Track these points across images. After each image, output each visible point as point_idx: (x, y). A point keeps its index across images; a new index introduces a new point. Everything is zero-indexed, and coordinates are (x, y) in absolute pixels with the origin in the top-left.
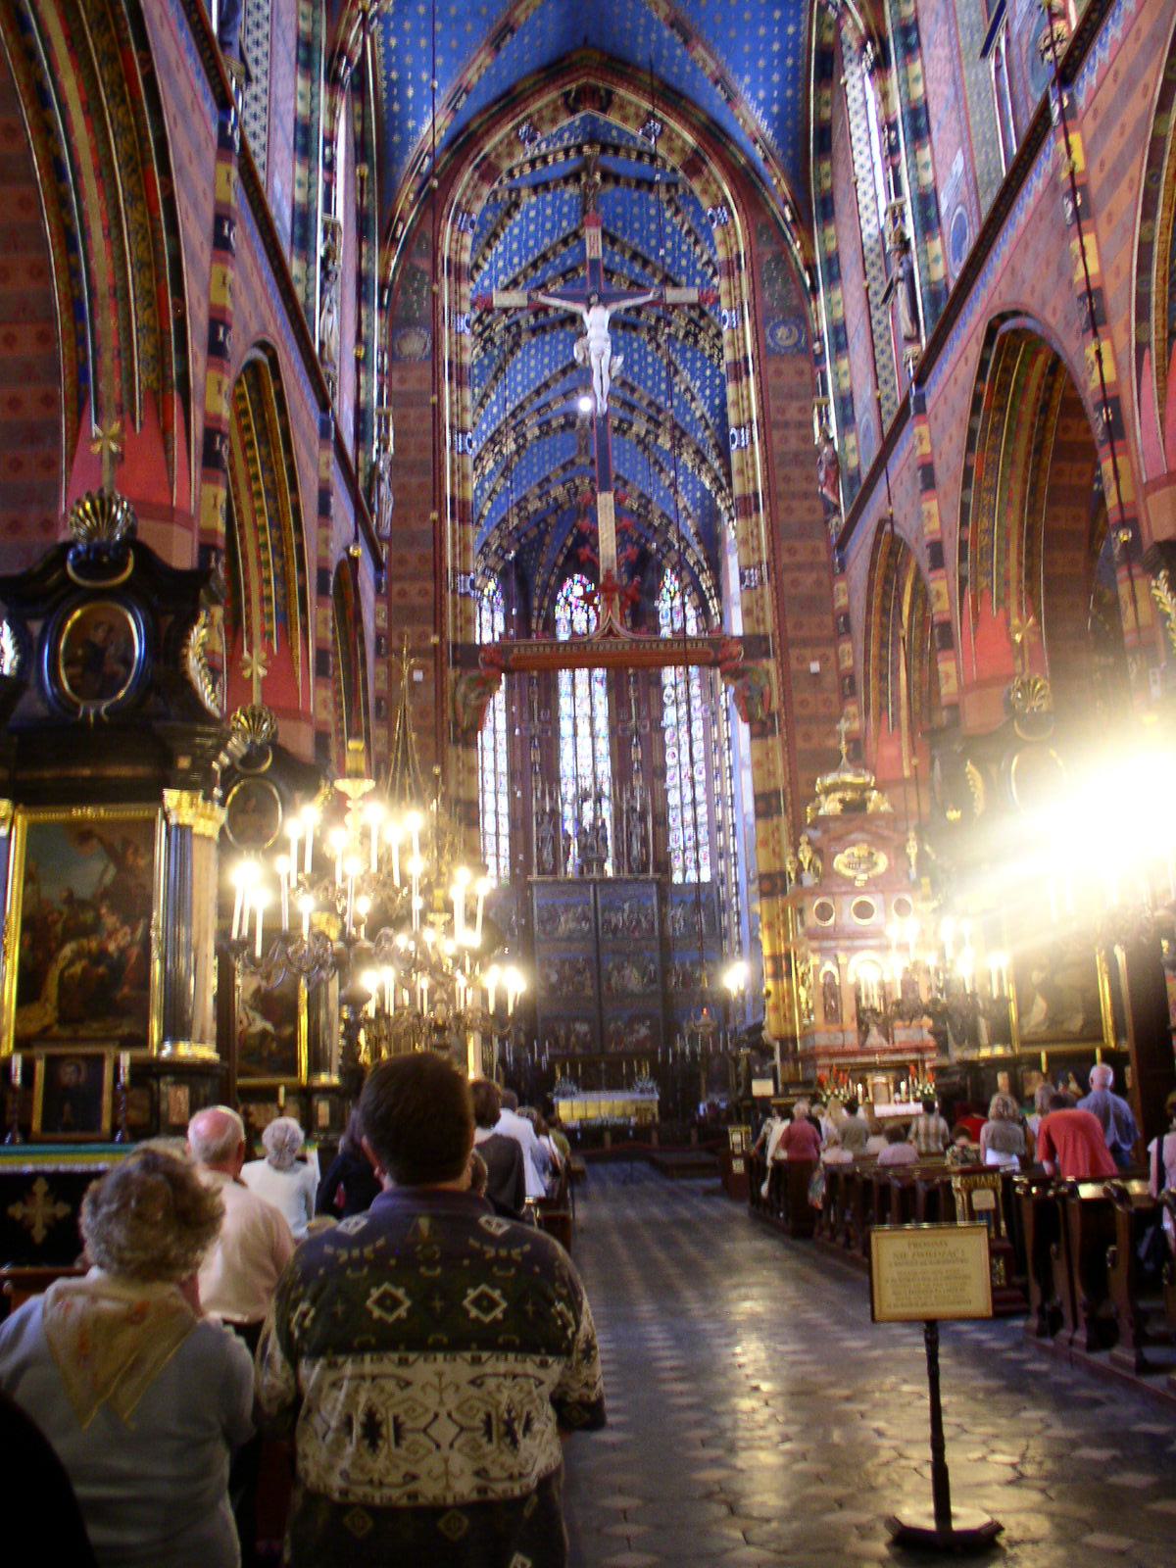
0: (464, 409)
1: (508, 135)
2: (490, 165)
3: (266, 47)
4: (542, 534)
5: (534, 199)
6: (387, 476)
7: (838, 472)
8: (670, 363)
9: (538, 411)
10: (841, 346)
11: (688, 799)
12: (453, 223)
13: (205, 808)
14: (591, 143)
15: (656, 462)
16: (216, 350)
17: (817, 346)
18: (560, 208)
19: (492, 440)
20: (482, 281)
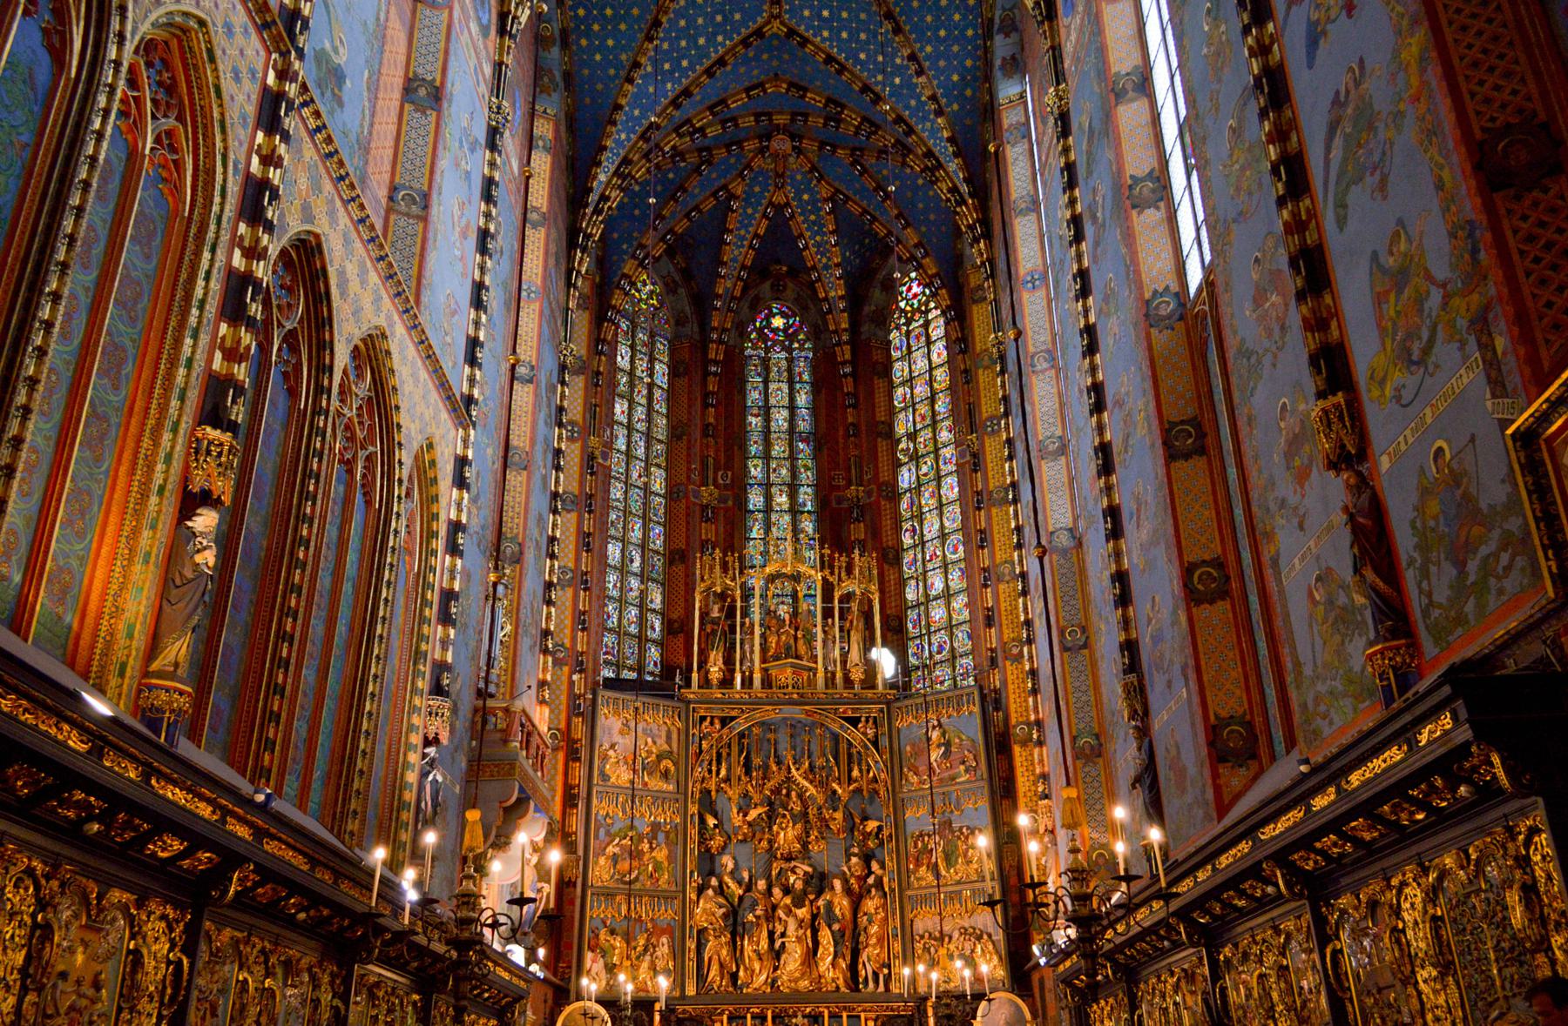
11: (938, 585)
15: (889, 16)
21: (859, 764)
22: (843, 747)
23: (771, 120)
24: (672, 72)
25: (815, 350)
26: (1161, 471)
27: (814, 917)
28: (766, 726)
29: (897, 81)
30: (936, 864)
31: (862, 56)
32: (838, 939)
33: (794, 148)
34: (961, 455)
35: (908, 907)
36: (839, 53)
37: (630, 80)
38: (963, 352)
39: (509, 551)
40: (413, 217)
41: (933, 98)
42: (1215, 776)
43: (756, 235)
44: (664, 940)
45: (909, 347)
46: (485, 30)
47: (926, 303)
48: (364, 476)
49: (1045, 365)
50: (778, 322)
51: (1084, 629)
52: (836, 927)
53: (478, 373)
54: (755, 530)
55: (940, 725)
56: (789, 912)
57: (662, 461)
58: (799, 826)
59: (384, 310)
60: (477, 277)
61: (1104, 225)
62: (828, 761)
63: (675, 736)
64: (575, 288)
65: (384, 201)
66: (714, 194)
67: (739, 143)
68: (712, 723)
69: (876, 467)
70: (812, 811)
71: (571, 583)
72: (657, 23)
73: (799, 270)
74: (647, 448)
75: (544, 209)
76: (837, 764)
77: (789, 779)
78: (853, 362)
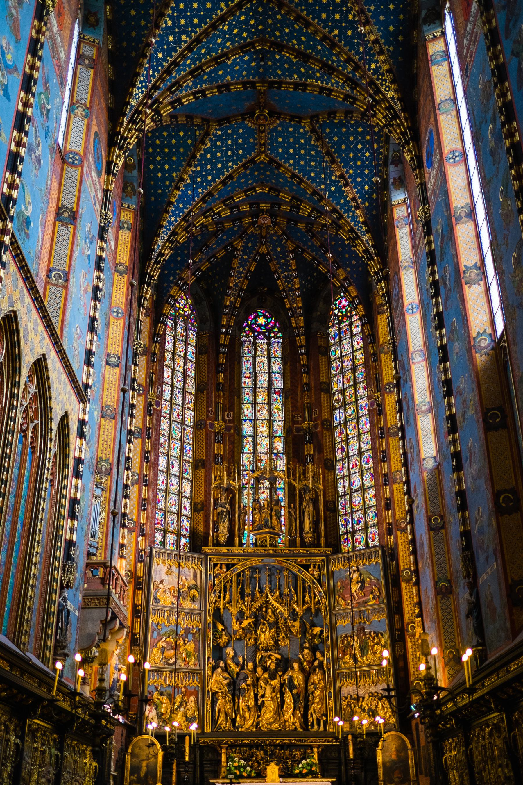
4: (230, 256)
9: (215, 59)
11: (357, 484)
15: (328, 153)
21: (309, 593)
22: (300, 583)
23: (259, 207)
24: (202, 182)
25: (283, 338)
26: (483, 437)
27: (282, 685)
28: (253, 569)
29: (333, 189)
30: (355, 654)
31: (313, 175)
32: (296, 698)
33: (272, 222)
34: (372, 404)
35: (338, 680)
36: (299, 172)
37: (178, 188)
38: (372, 343)
39: (104, 468)
40: (60, 286)
41: (354, 199)
42: (511, 614)
43: (249, 271)
44: (192, 698)
45: (340, 337)
46: (99, 175)
47: (351, 312)
48: (32, 437)
49: (420, 359)
50: (261, 321)
51: (442, 517)
52: (295, 691)
53: (91, 370)
54: (247, 447)
55: (358, 570)
56: (267, 682)
57: (191, 406)
58: (273, 630)
59: (45, 344)
60: (92, 314)
61: (450, 290)
62: (290, 590)
63: (199, 575)
64: (143, 307)
65: (44, 278)
66: (225, 248)
67: (240, 220)
68: (221, 568)
69: (320, 411)
70: (281, 622)
71: (137, 482)
72: (194, 157)
73: (274, 289)
74: (183, 398)
75: (127, 264)
76: (296, 593)
77: (267, 602)
78: (307, 346)
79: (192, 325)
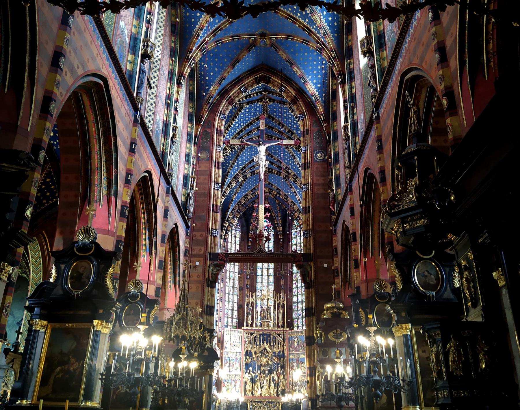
0: (219, 176)
1: (237, 91)
2: (231, 99)
3: (157, 78)
5: (248, 106)
6: (192, 197)
7: (335, 201)
8: (293, 155)
9: (250, 168)
10: (337, 161)
12: (219, 117)
13: (106, 325)
14: (265, 91)
16: (127, 182)
17: (330, 159)
18: (256, 108)
19: (235, 177)
20: (231, 130)
41: (299, 200)
45: (296, 235)
79: (238, 228)
